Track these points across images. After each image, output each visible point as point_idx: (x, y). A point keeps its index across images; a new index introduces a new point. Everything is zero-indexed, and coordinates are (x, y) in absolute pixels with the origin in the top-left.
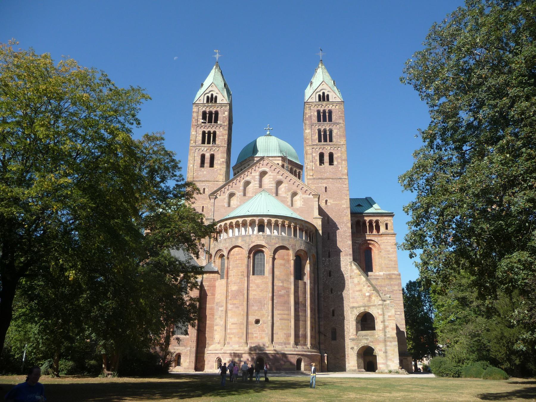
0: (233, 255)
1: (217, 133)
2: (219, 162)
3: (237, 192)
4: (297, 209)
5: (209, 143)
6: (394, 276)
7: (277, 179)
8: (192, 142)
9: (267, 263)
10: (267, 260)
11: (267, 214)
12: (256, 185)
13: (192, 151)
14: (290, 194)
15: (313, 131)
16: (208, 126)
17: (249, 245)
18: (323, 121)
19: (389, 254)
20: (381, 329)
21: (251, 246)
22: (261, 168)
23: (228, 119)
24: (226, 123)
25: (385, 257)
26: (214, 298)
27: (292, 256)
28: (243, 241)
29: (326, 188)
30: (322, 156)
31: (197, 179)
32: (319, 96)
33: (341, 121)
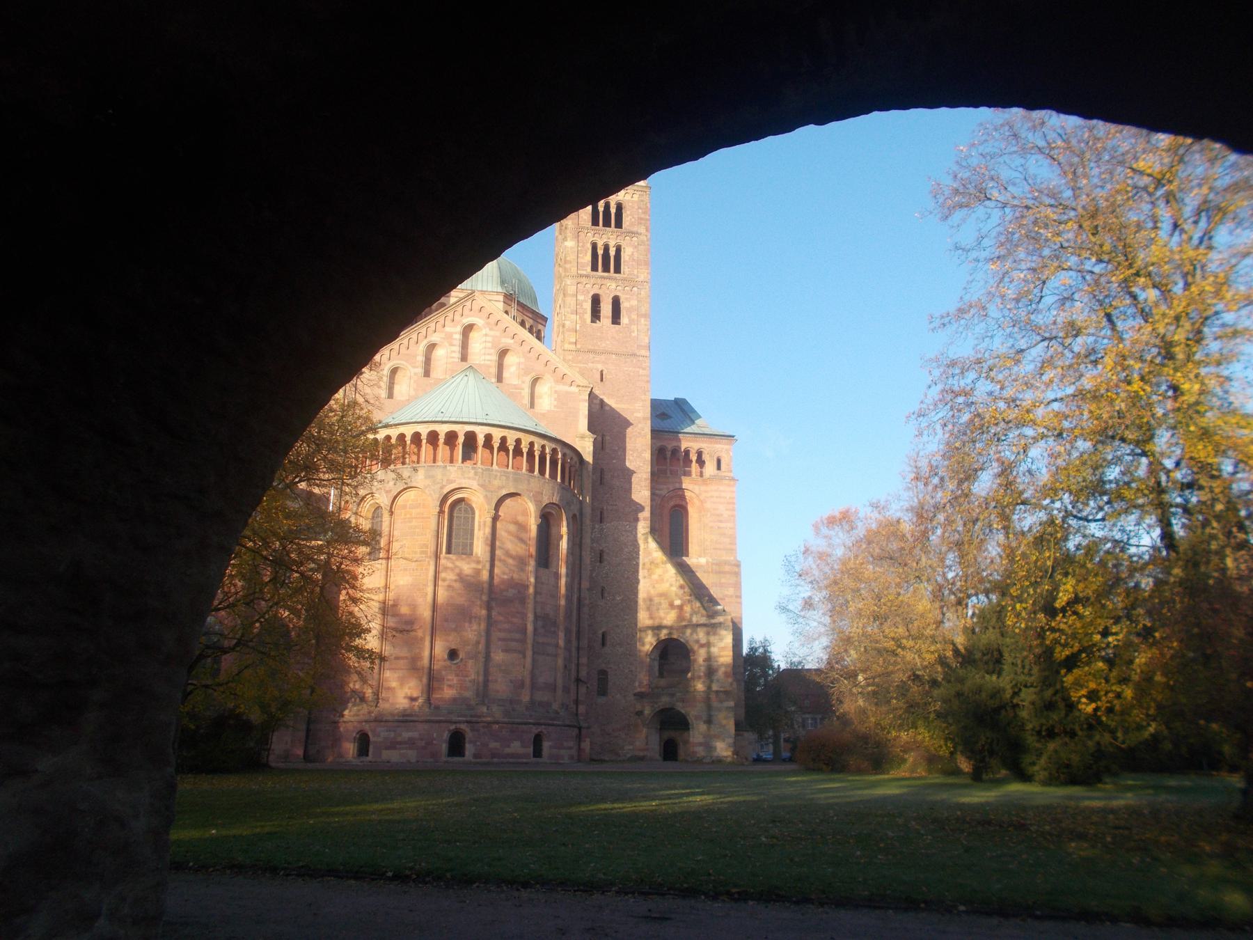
0: (404, 507)
3: (410, 367)
4: (543, 415)
6: (727, 568)
7: (501, 346)
9: (479, 530)
10: (479, 522)
11: (485, 421)
12: (454, 355)
14: (528, 380)
15: (581, 244)
17: (442, 488)
18: (604, 226)
19: (721, 521)
20: (702, 674)
21: (445, 491)
25: (712, 527)
27: (533, 515)
28: (426, 478)
30: (596, 300)
33: (642, 230)
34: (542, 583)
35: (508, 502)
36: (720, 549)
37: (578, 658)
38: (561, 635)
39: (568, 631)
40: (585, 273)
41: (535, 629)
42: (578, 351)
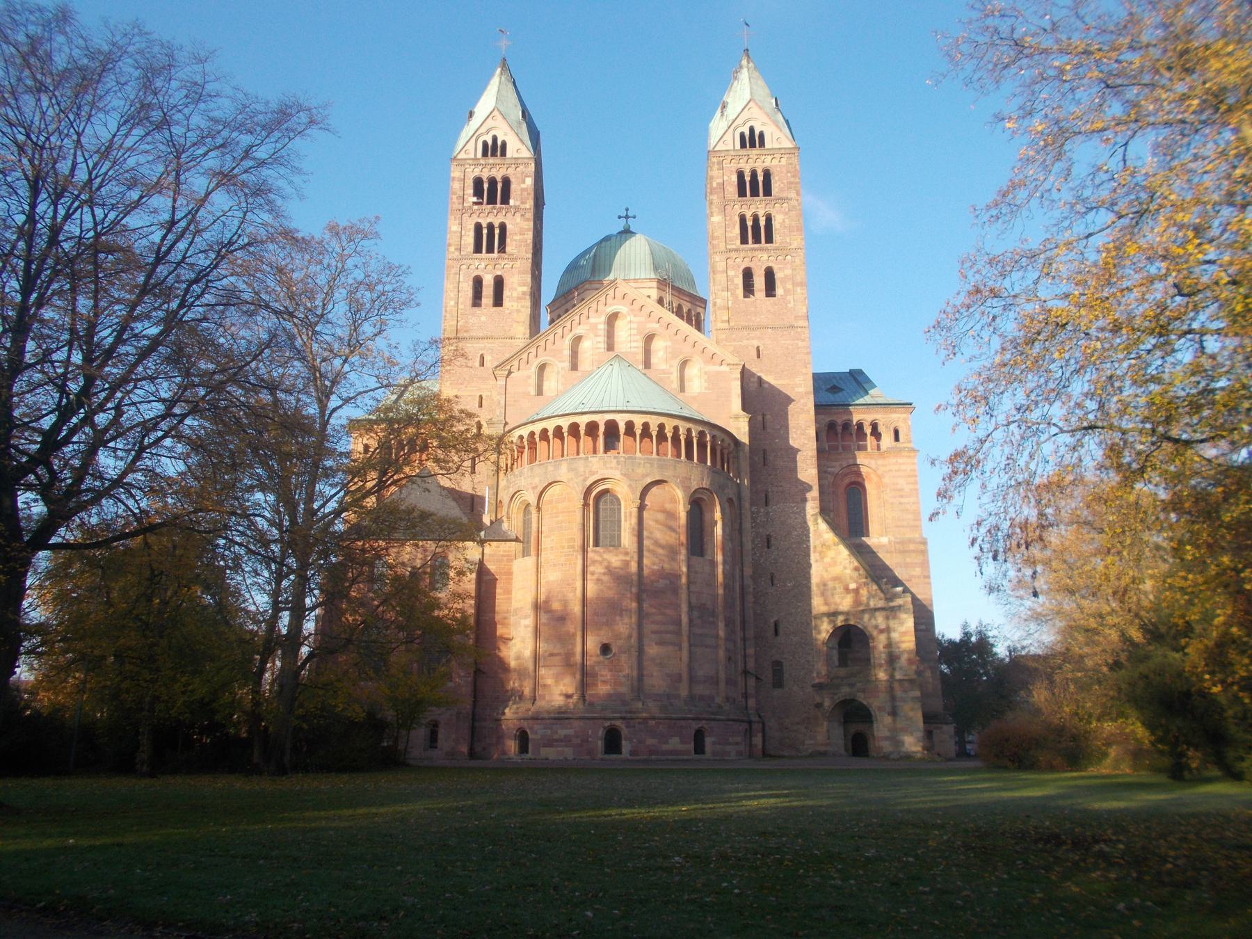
0: (551, 502)
1: (509, 227)
2: (515, 294)
5: (490, 250)
6: (912, 547)
7: (646, 332)
8: (452, 249)
9: (626, 520)
13: (453, 271)
14: (676, 364)
15: (728, 218)
16: (487, 211)
19: (902, 497)
21: (588, 483)
22: (611, 305)
23: (532, 193)
24: (530, 204)
25: (892, 504)
26: (510, 599)
27: (682, 502)
28: (569, 471)
29: (758, 349)
31: (465, 335)
32: (742, 135)
34: (696, 572)
35: (654, 490)
36: (903, 526)
37: (745, 649)
38: (721, 625)
39: (729, 623)
40: (734, 247)
41: (691, 621)
42: (731, 329)
